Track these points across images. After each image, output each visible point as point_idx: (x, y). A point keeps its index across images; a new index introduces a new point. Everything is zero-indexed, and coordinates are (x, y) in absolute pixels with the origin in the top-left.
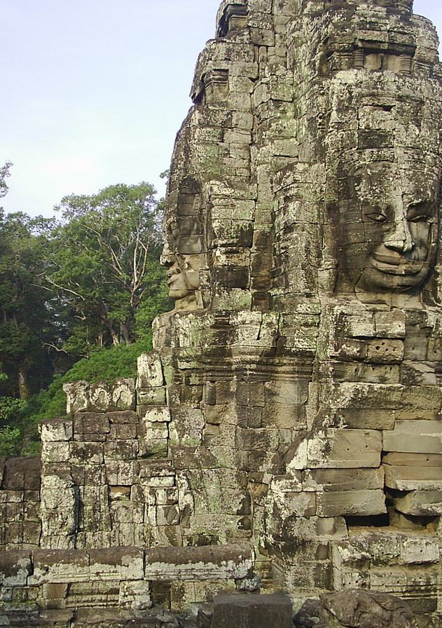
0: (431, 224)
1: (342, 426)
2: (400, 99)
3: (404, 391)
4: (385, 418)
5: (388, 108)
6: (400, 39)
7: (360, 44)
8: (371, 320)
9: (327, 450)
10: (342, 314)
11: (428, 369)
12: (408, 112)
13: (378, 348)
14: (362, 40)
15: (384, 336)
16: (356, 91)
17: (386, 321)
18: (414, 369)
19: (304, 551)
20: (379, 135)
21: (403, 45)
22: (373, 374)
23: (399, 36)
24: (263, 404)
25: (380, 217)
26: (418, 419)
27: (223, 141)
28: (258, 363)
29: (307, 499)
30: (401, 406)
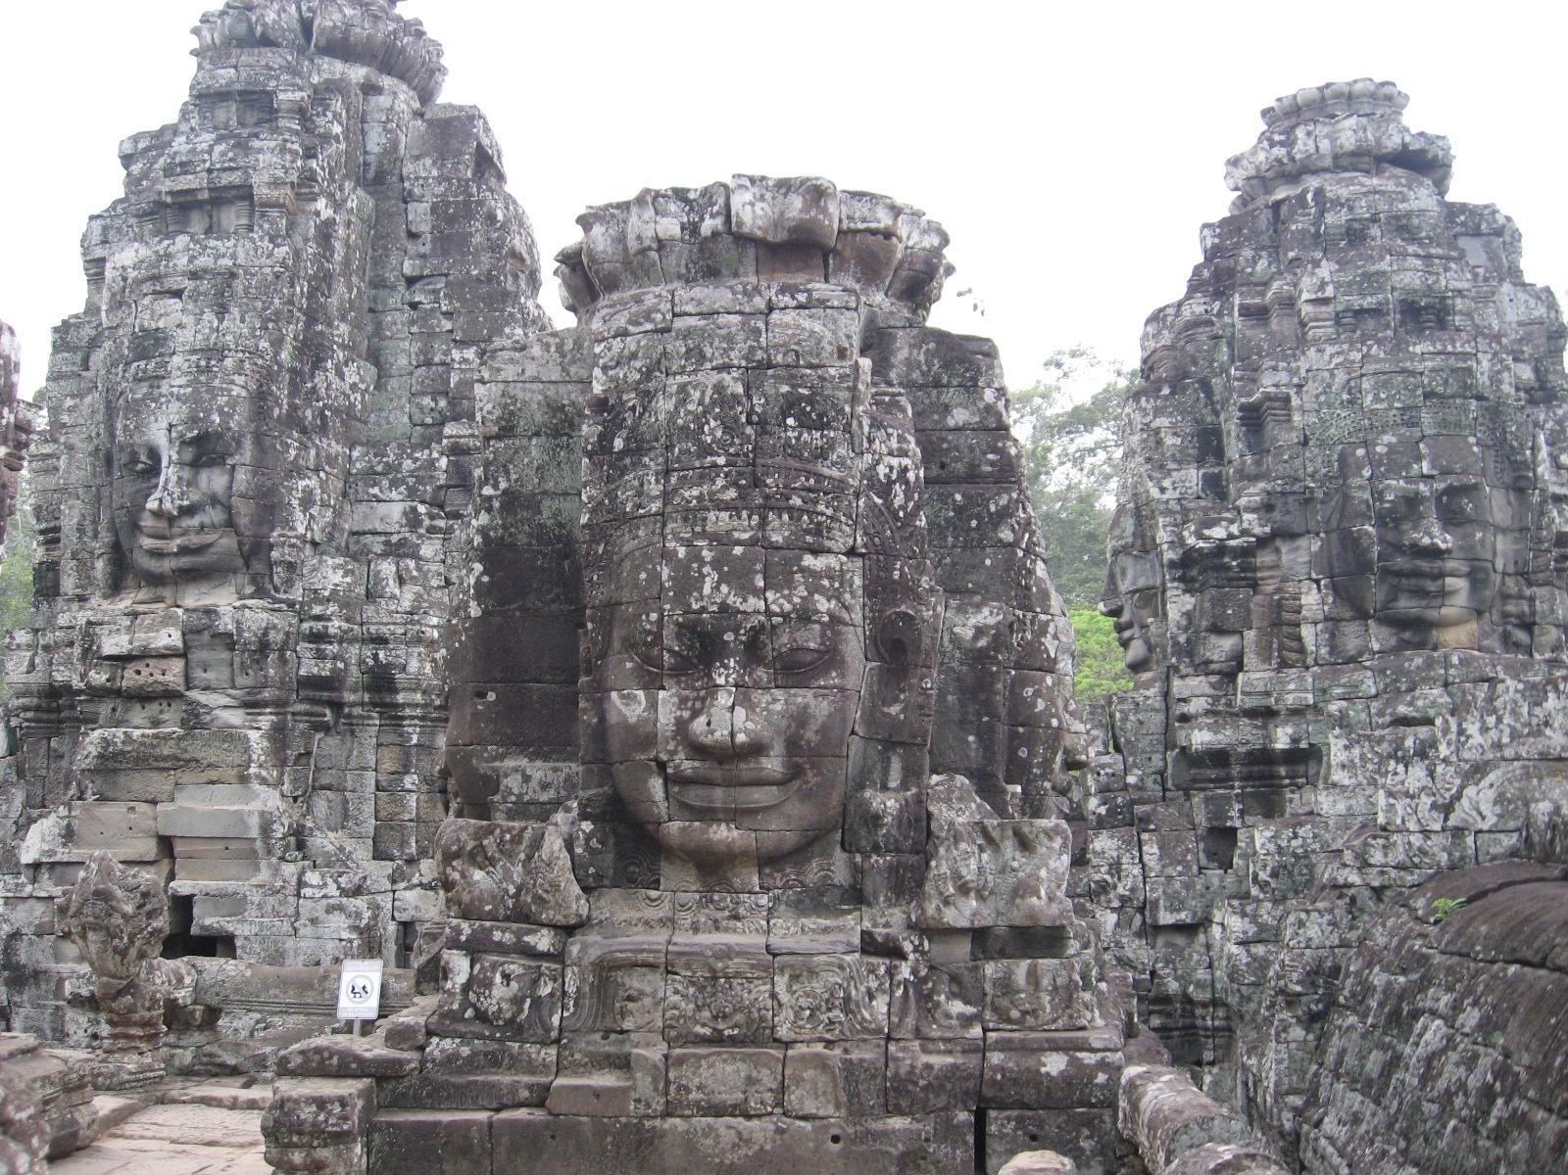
0: (233, 467)
1: (90, 798)
2: (194, 275)
3: (180, 738)
4: (159, 783)
5: (177, 294)
6: (226, 179)
7: (169, 200)
8: (129, 629)
9: (69, 835)
10: (90, 623)
11: (225, 700)
12: (206, 295)
13: (138, 673)
14: (171, 193)
15: (143, 655)
16: (132, 274)
17: (150, 629)
18: (198, 704)
19: (38, 985)
20: (157, 340)
21: (231, 187)
22: (139, 715)
23: (224, 175)
24: (44, 772)
25: (140, 466)
26: (213, 783)
27: (87, 369)
28: (37, 709)
29: (39, 909)
30: (181, 763)
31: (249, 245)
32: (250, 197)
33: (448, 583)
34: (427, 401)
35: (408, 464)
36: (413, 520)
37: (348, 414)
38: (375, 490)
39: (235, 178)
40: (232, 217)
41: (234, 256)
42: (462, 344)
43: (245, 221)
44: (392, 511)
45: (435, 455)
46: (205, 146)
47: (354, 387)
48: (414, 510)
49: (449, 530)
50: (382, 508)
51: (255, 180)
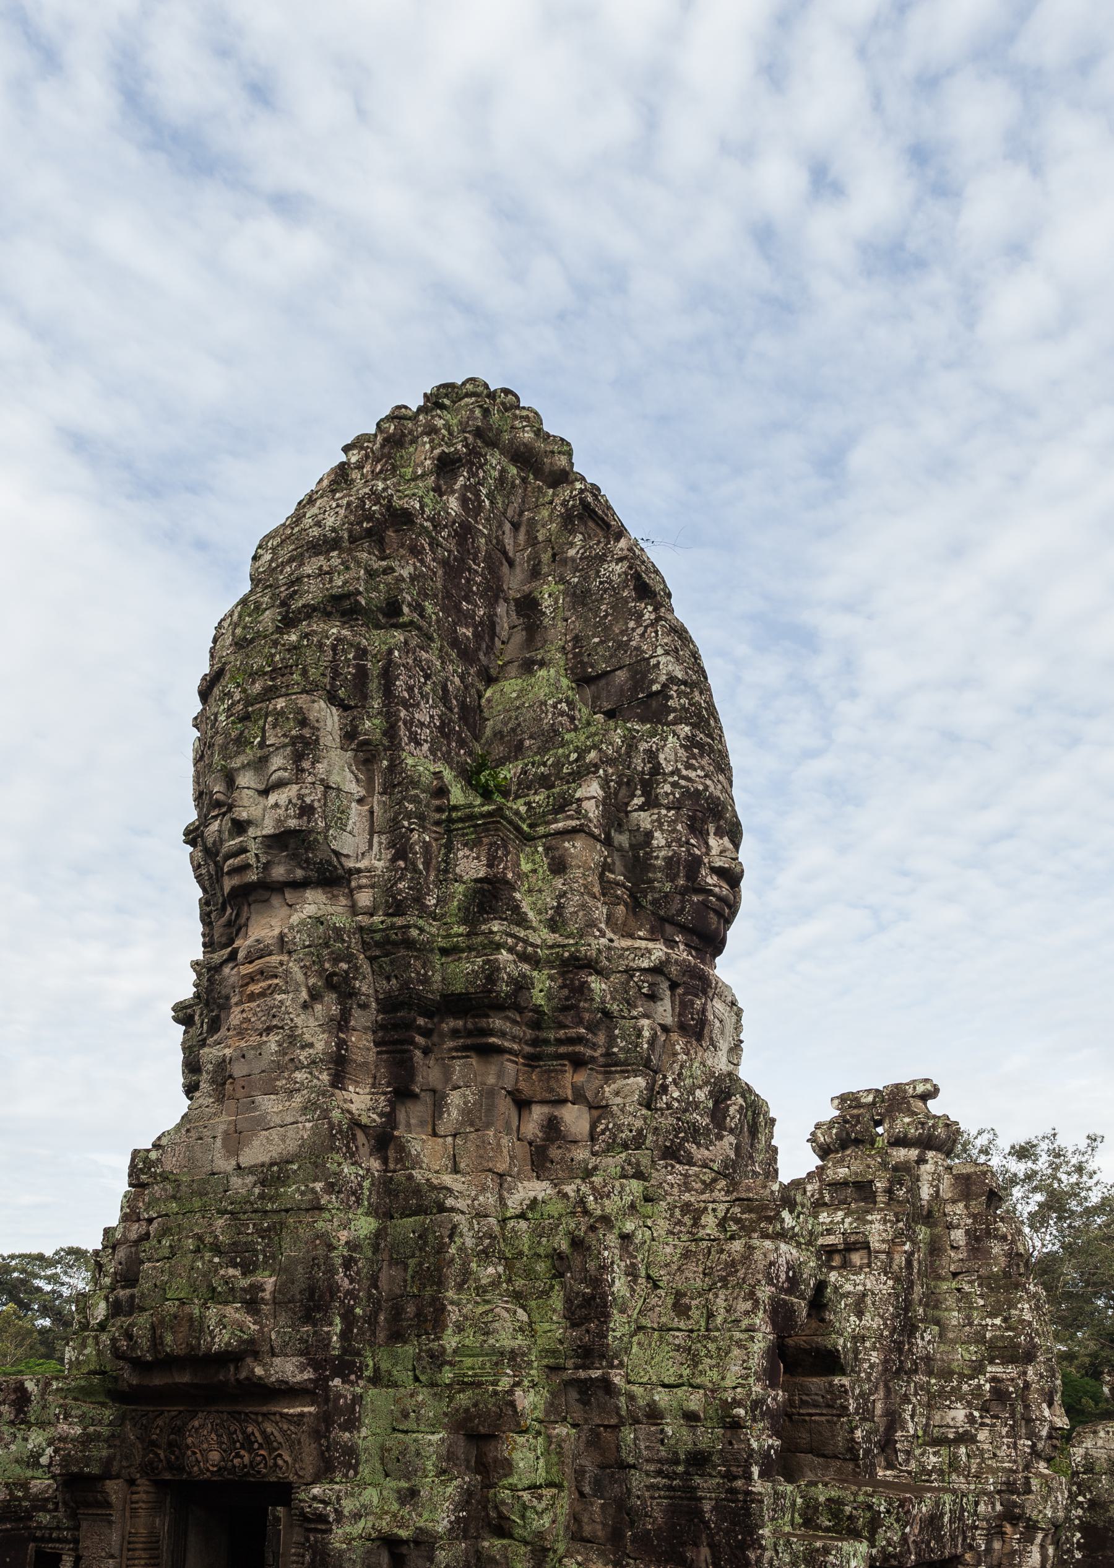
6: (852, 1239)
31: (872, 1278)
32: (869, 1248)
33: (995, 1455)
34: (973, 1348)
35: (965, 1387)
36: (971, 1419)
37: (928, 1359)
38: (948, 1403)
39: (860, 1238)
40: (857, 1258)
41: (865, 1285)
42: (992, 1315)
43: (866, 1261)
44: (958, 1414)
45: (982, 1382)
46: (839, 1219)
47: (929, 1342)
48: (971, 1414)
49: (994, 1425)
50: (952, 1413)
51: (871, 1239)
